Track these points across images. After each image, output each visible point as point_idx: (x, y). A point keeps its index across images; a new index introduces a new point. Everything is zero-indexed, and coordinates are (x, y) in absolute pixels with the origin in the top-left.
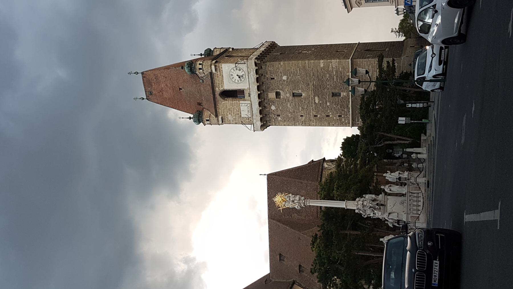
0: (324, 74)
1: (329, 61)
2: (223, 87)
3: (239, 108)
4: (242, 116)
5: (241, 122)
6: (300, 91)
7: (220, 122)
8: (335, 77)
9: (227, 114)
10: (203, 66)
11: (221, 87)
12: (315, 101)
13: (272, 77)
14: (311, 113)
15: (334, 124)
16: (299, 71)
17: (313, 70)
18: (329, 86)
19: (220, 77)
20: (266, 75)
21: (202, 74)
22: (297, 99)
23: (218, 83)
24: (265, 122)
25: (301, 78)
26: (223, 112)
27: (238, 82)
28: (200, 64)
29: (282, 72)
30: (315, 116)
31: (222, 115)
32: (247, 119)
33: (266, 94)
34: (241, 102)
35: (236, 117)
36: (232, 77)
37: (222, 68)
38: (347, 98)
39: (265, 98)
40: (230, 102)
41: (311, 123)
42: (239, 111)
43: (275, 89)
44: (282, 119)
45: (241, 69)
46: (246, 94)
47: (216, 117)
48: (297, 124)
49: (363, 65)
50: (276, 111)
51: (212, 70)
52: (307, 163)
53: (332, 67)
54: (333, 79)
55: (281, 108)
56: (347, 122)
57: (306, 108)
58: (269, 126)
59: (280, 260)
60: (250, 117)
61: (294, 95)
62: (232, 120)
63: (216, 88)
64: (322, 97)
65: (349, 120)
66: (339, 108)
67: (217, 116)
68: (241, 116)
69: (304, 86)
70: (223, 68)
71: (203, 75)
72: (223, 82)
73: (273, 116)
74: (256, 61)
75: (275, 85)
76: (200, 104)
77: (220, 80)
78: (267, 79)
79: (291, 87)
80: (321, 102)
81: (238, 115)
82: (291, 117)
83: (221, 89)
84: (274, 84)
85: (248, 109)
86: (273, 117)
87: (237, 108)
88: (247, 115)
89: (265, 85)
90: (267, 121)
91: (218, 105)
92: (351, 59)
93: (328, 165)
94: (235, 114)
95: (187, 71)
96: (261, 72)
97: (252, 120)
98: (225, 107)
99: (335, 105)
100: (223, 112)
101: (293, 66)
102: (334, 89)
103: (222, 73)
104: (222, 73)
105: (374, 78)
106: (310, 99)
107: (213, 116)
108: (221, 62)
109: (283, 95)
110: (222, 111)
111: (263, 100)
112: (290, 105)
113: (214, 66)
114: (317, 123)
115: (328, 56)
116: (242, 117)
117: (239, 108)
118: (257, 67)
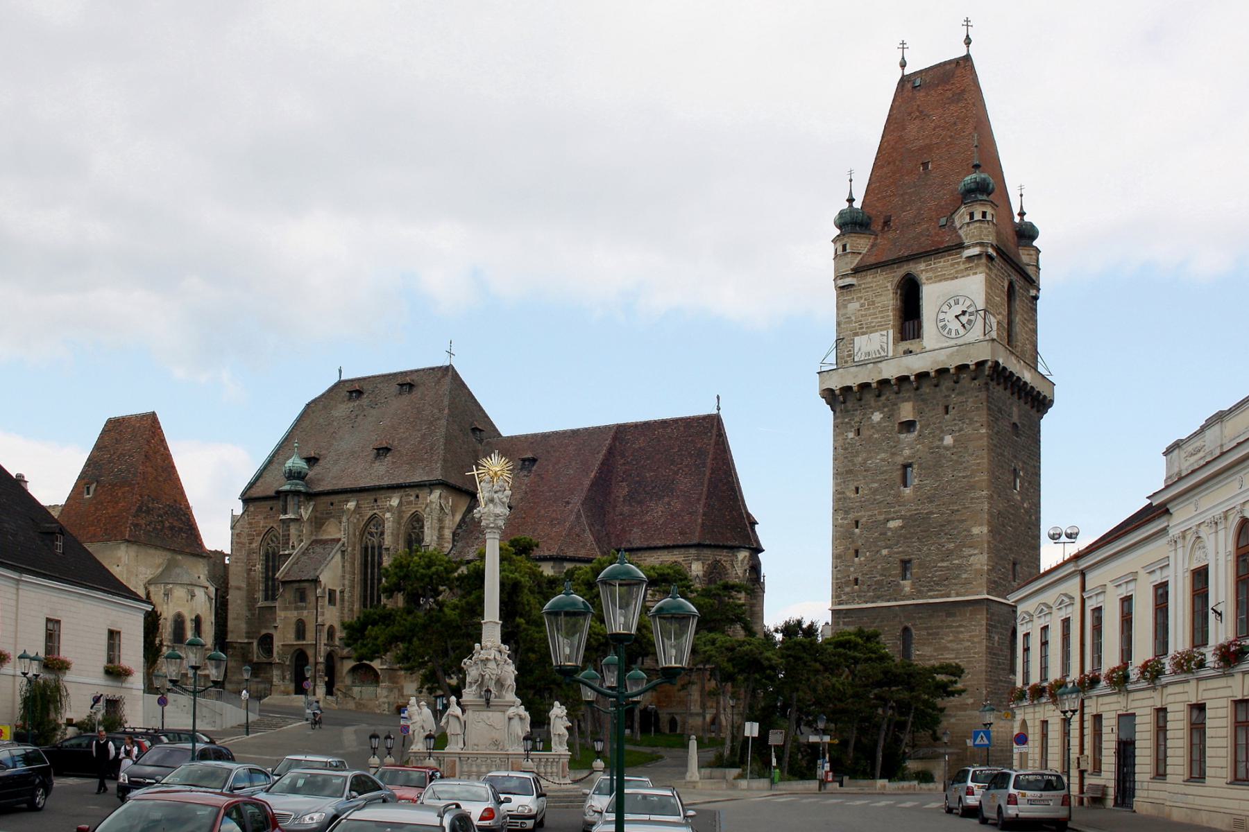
0: (955, 538)
1: (986, 546)
4: (856, 338)
6: (916, 480)
7: (841, 283)
8: (945, 564)
9: (861, 298)
10: (978, 225)
12: (893, 519)
14: (863, 513)
15: (839, 568)
17: (964, 511)
20: (956, 391)
21: (961, 222)
22: (897, 474)
24: (841, 398)
28: (984, 214)
29: (962, 432)
30: (857, 523)
31: (859, 285)
32: (850, 351)
33: (909, 397)
34: (891, 332)
35: (856, 322)
36: (953, 304)
38: (897, 593)
39: (901, 395)
40: (892, 302)
41: (841, 515)
44: (848, 441)
46: (911, 344)
47: (852, 270)
48: (839, 481)
51: (968, 247)
53: (971, 556)
54: (943, 561)
56: (844, 597)
57: (875, 500)
58: (832, 410)
59: (524, 460)
61: (906, 467)
63: (924, 264)
64: (900, 536)
65: (846, 604)
66: (875, 579)
67: (856, 271)
68: (856, 334)
71: (957, 224)
72: (940, 281)
73: (857, 419)
74: (990, 363)
76: (886, 223)
78: (946, 396)
80: (889, 534)
81: (860, 328)
82: (854, 465)
83: (923, 277)
88: (860, 349)
90: (844, 402)
92: (988, 599)
93: (743, 561)
96: (964, 378)
97: (846, 365)
99: (884, 569)
101: (975, 460)
102: (920, 564)
105: (942, 654)
106: (897, 508)
107: (856, 262)
108: (990, 269)
110: (870, 283)
111: (896, 388)
112: (883, 460)
113: (978, 253)
114: (841, 529)
115: (1001, 542)
116: (854, 340)
118: (974, 367)
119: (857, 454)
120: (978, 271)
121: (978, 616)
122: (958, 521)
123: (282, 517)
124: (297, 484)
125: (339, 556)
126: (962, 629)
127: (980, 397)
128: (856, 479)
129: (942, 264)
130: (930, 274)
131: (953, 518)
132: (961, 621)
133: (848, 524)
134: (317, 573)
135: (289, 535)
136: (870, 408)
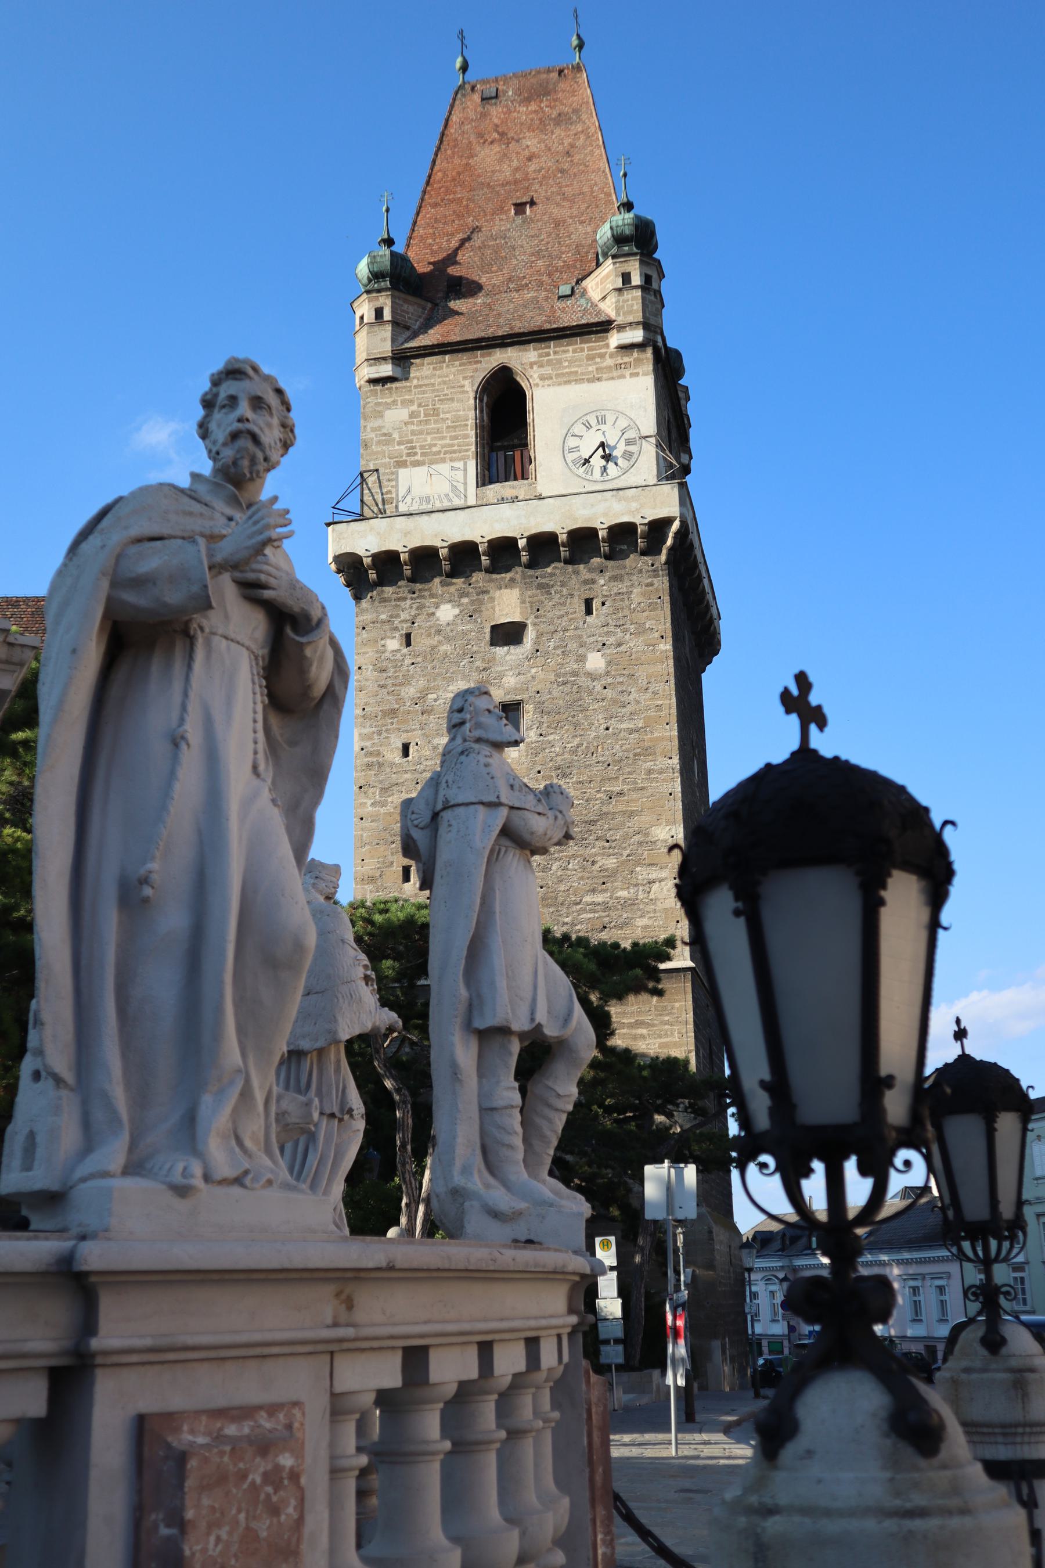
2: (541, 383)
3: (442, 455)
4: (403, 472)
5: (372, 468)
8: (599, 898)
11: (543, 371)
13: (596, 604)
16: (632, 726)
18: (559, 873)
19: (590, 369)
20: (607, 575)
21: (602, 291)
23: (560, 361)
25: (597, 738)
26: (421, 386)
27: (571, 450)
29: (623, 648)
33: (512, 580)
35: (400, 443)
36: (593, 422)
37: (632, 375)
40: (471, 414)
42: (426, 459)
43: (537, 617)
44: (387, 655)
45: (633, 460)
46: (513, 487)
49: (667, 1027)
50: (431, 627)
51: (621, 328)
54: (593, 891)
55: (443, 648)
60: (397, 507)
62: (380, 428)
63: (536, 353)
68: (402, 464)
69: (557, 755)
70: (635, 379)
73: (404, 616)
75: (560, 617)
77: (573, 370)
78: (586, 582)
79: (550, 693)
81: (409, 455)
82: (400, 700)
83: (535, 374)
84: (562, 612)
85: (439, 496)
86: (398, 616)
87: (443, 447)
88: (409, 491)
89: (557, 571)
91: (457, 363)
94: (415, 438)
95: (617, 221)
98: (446, 392)
100: (421, 386)
101: (652, 699)
103: (611, 375)
104: (611, 375)
109: (508, 658)
117: (442, 455)
119: (406, 681)
120: (640, 370)
121: (677, 1005)
122: (624, 813)
126: (644, 1031)
127: (656, 585)
128: (404, 727)
129: (570, 354)
130: (547, 370)
131: (611, 808)
132: (640, 1013)
133: (390, 814)
136: (432, 596)
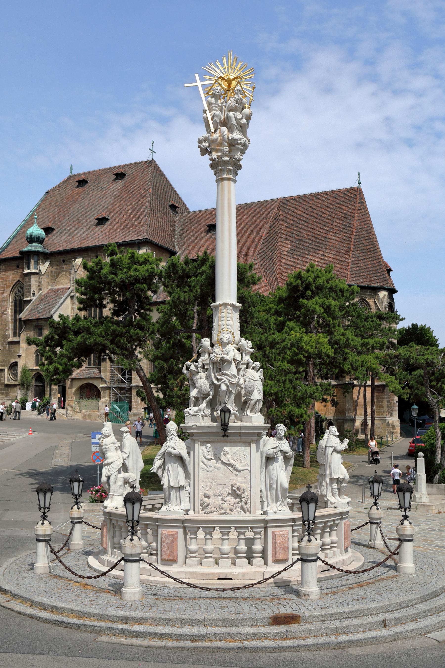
52: (385, 260)
93: (384, 298)
123: (26, 271)
124: (36, 246)
125: (69, 299)
134: (52, 313)
135: (30, 285)
